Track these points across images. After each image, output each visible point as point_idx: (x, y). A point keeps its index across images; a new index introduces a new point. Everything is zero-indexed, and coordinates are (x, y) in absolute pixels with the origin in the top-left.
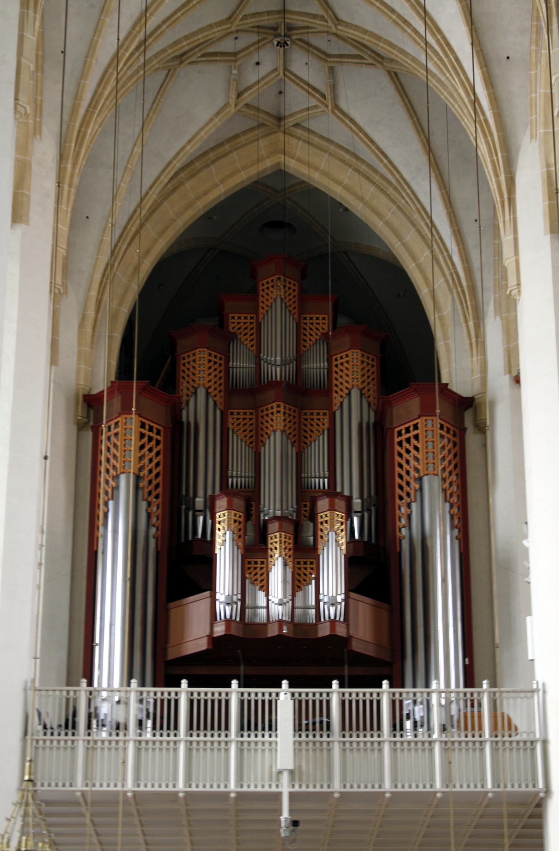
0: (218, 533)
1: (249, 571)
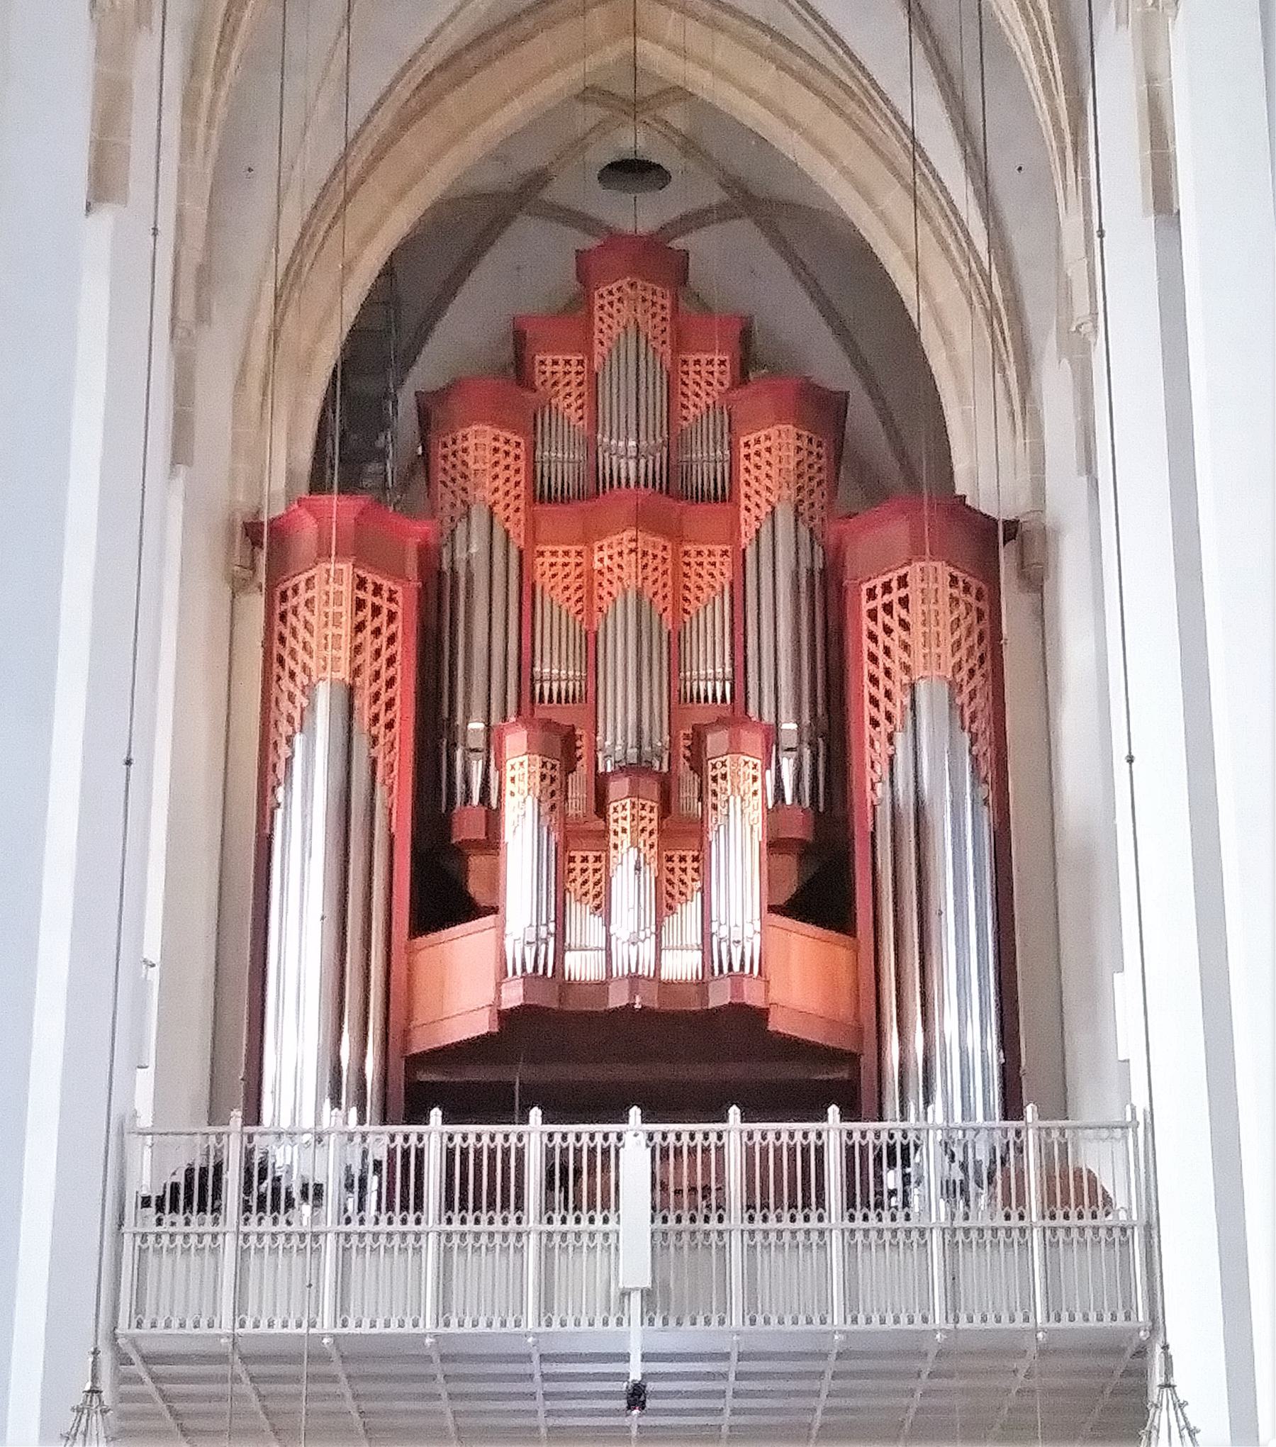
0: (508, 800)
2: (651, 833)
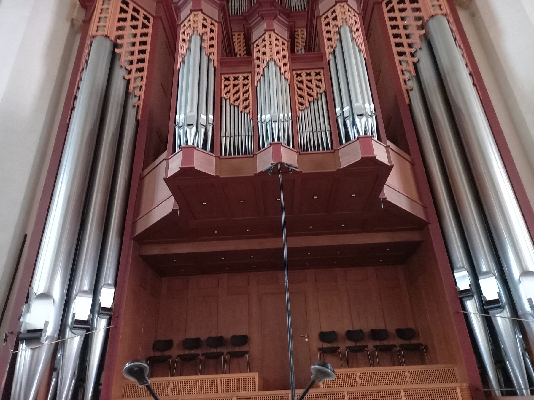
1: (227, 89)
2: (284, 57)
